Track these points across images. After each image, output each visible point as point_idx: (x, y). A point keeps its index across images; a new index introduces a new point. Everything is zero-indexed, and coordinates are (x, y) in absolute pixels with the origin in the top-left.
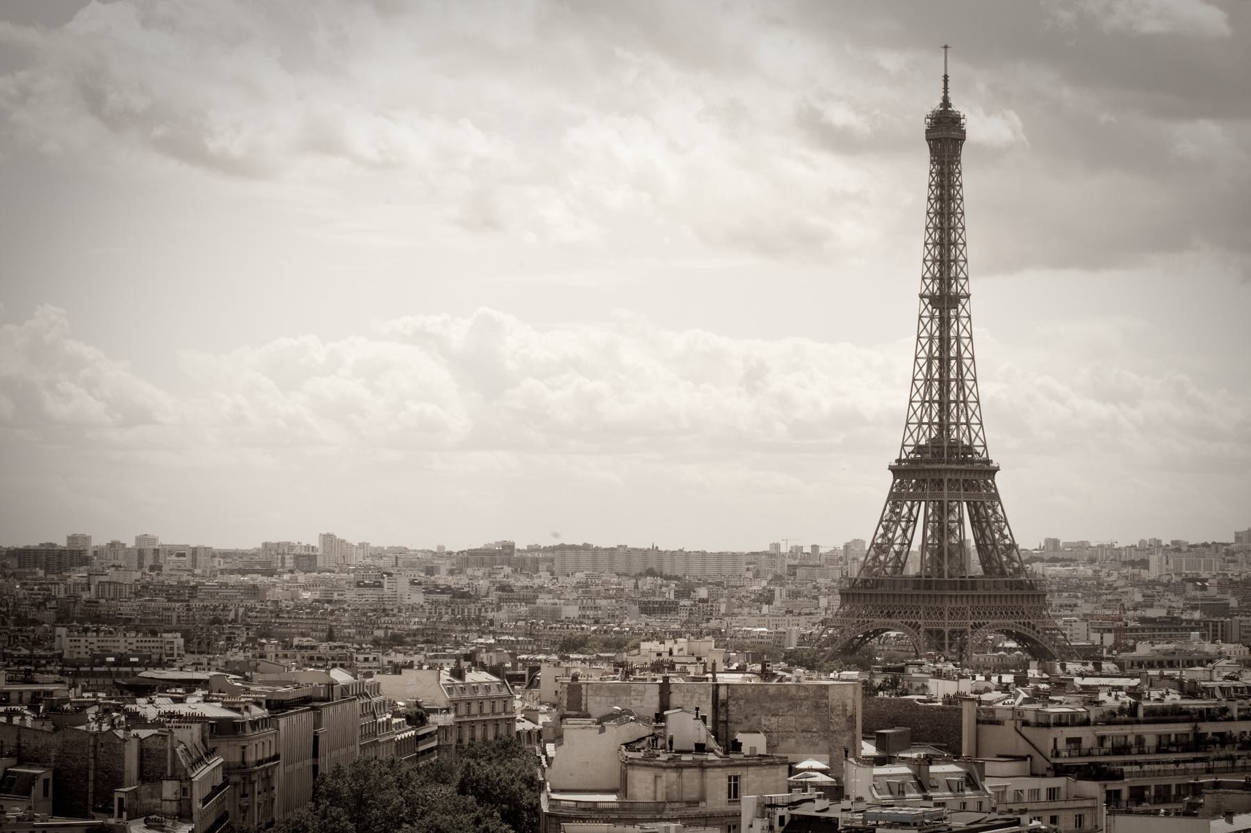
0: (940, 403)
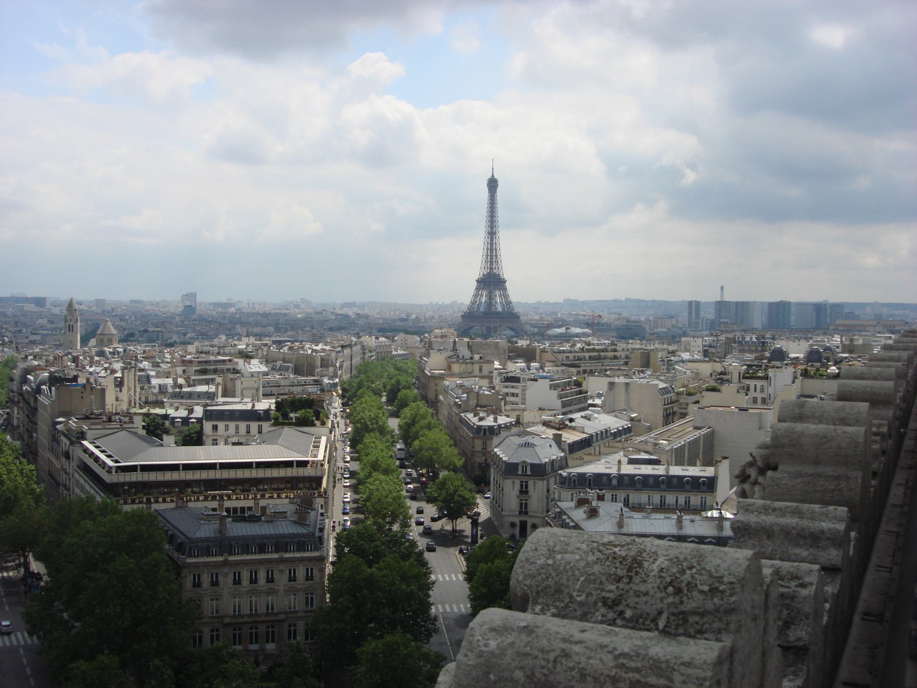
0: (490, 262)
